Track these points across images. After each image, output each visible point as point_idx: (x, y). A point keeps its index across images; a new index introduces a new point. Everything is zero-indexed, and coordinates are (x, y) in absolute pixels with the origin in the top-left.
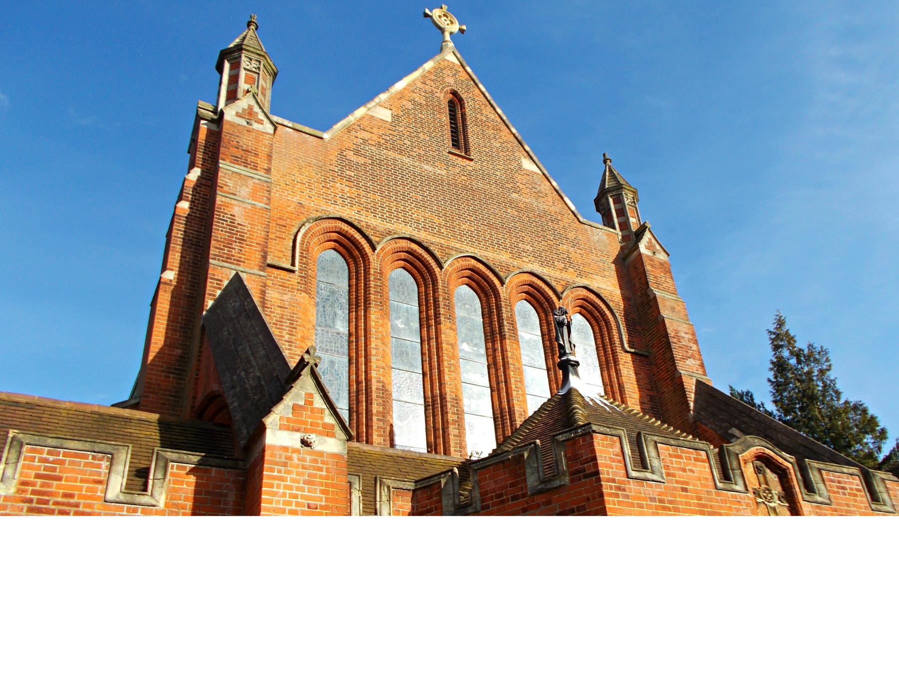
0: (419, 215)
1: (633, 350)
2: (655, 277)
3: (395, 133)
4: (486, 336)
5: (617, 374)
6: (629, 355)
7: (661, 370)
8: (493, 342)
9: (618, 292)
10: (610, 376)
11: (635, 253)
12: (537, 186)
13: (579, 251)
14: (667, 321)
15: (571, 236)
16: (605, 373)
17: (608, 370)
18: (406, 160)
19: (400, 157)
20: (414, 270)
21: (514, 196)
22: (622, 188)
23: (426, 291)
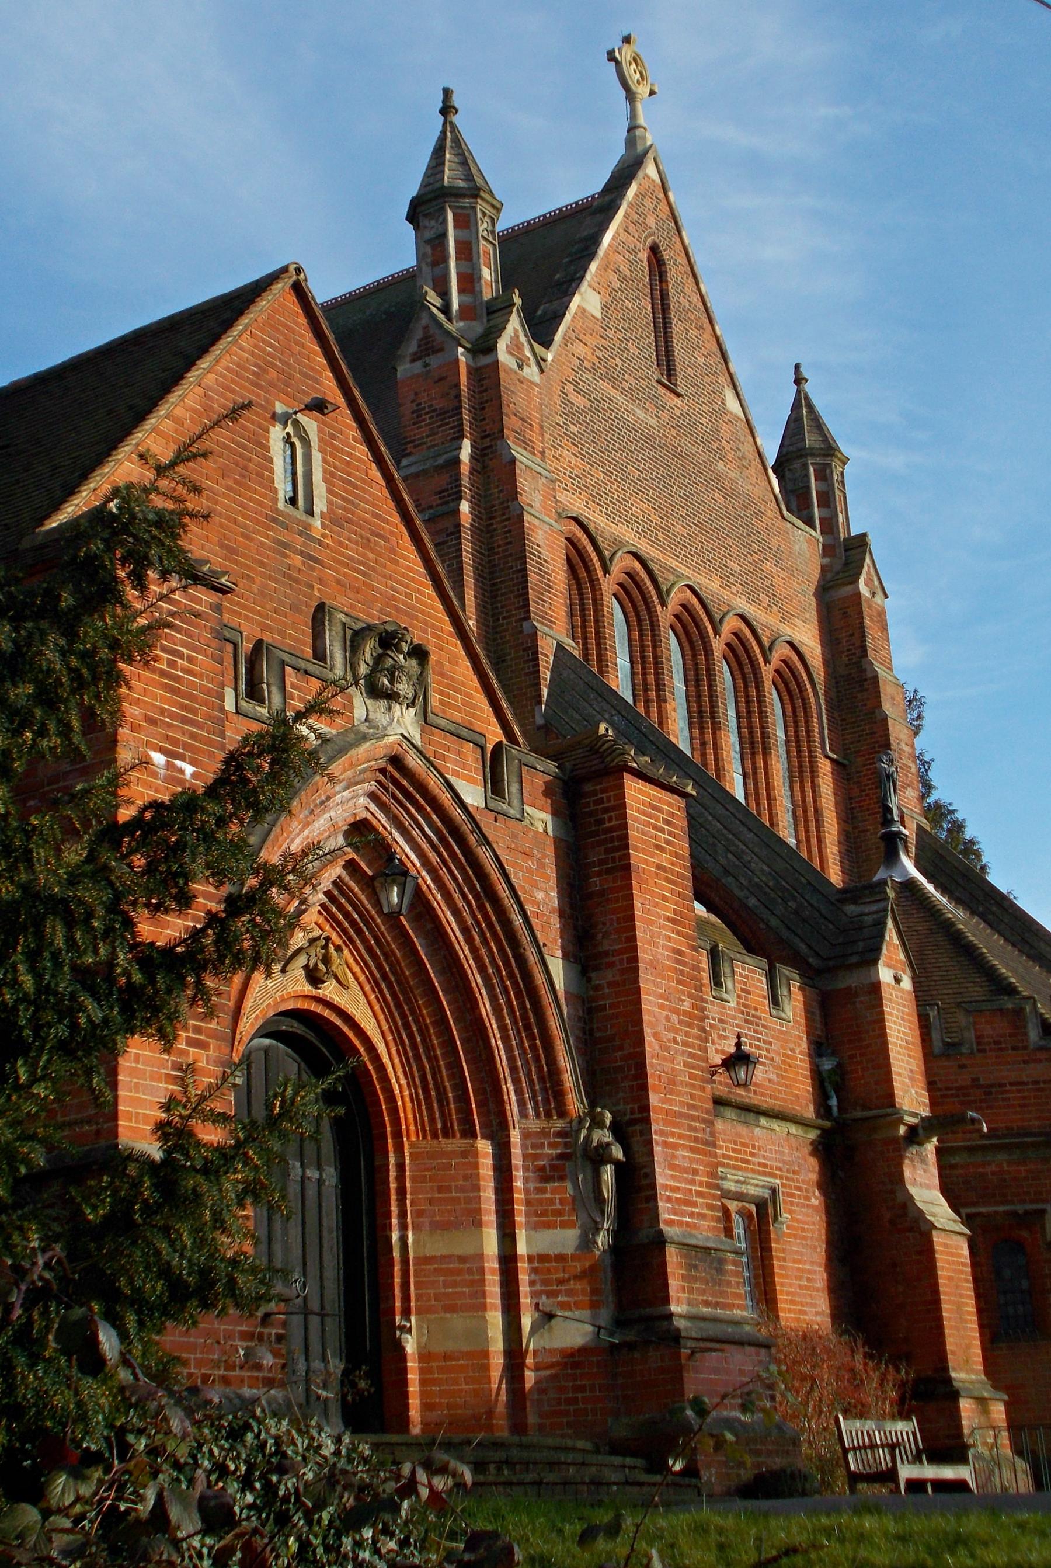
0: (638, 507)
1: (835, 756)
2: (874, 639)
3: (606, 343)
4: (690, 718)
5: (814, 791)
6: (828, 762)
7: (867, 795)
8: (702, 729)
9: (818, 650)
10: (803, 792)
11: (848, 589)
12: (740, 446)
13: (783, 574)
14: (890, 722)
15: (774, 544)
16: (797, 787)
17: (802, 782)
18: (620, 398)
19: (613, 392)
20: (630, 609)
21: (720, 465)
22: (833, 455)
23: (641, 640)
